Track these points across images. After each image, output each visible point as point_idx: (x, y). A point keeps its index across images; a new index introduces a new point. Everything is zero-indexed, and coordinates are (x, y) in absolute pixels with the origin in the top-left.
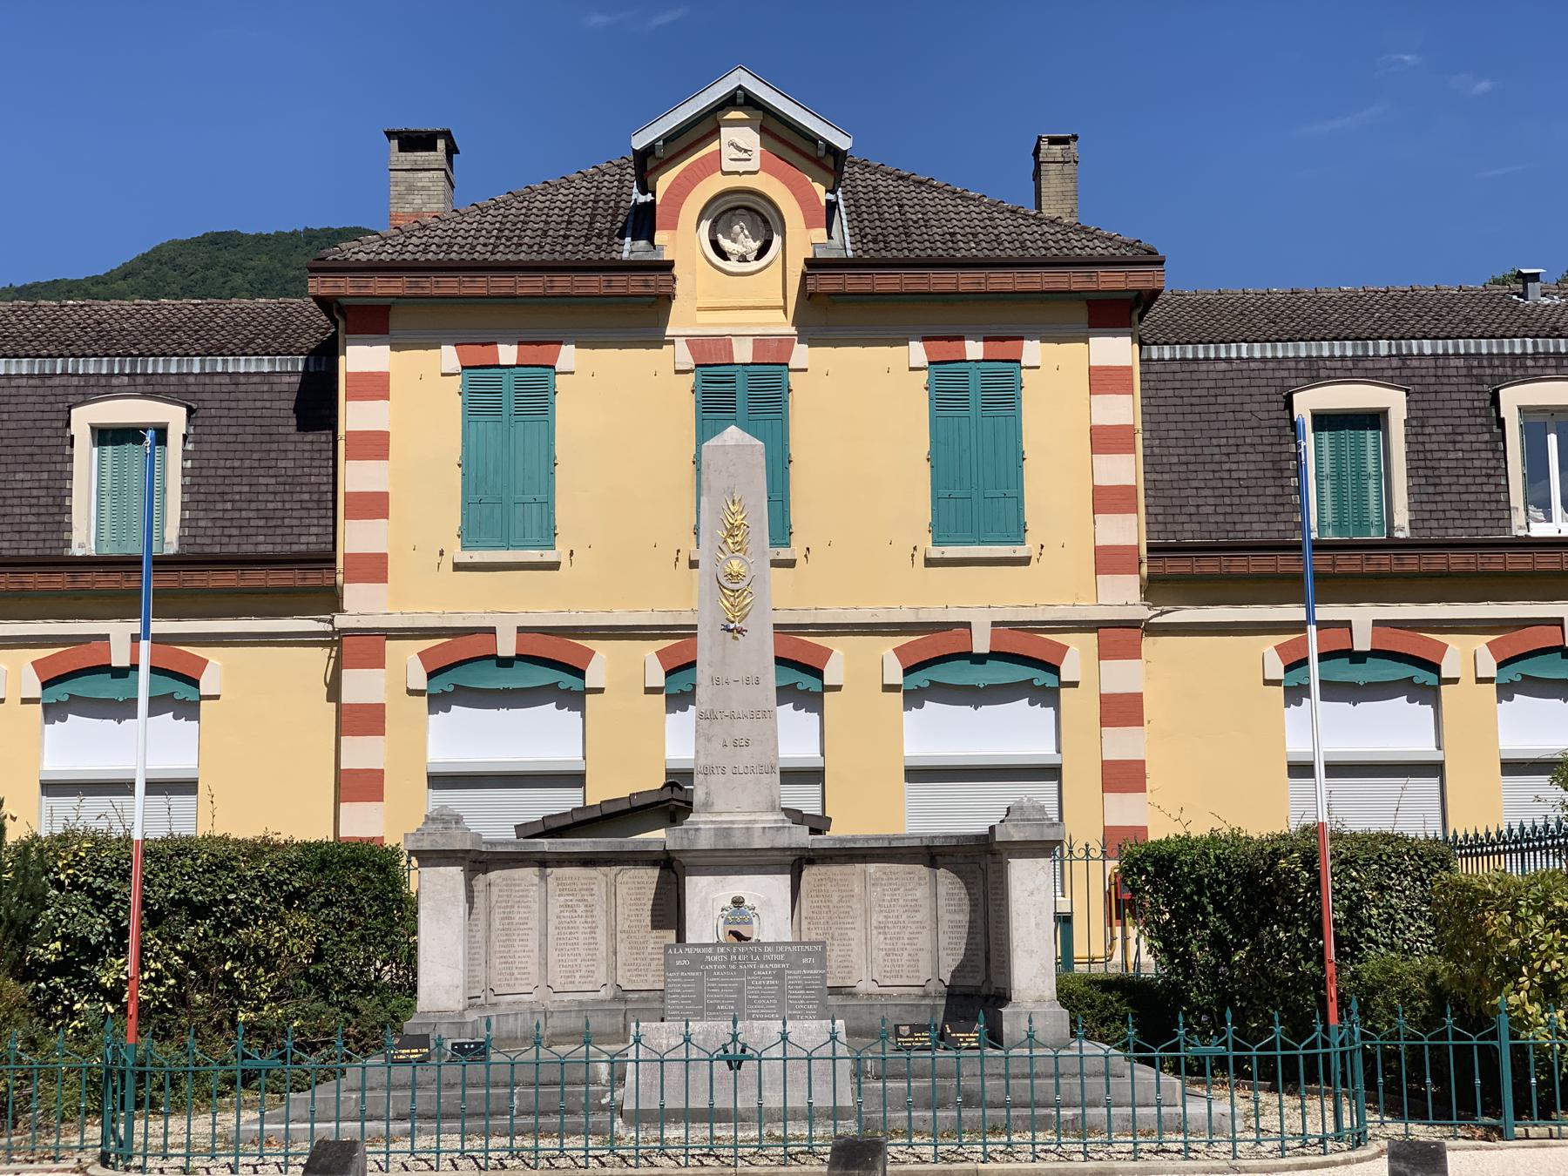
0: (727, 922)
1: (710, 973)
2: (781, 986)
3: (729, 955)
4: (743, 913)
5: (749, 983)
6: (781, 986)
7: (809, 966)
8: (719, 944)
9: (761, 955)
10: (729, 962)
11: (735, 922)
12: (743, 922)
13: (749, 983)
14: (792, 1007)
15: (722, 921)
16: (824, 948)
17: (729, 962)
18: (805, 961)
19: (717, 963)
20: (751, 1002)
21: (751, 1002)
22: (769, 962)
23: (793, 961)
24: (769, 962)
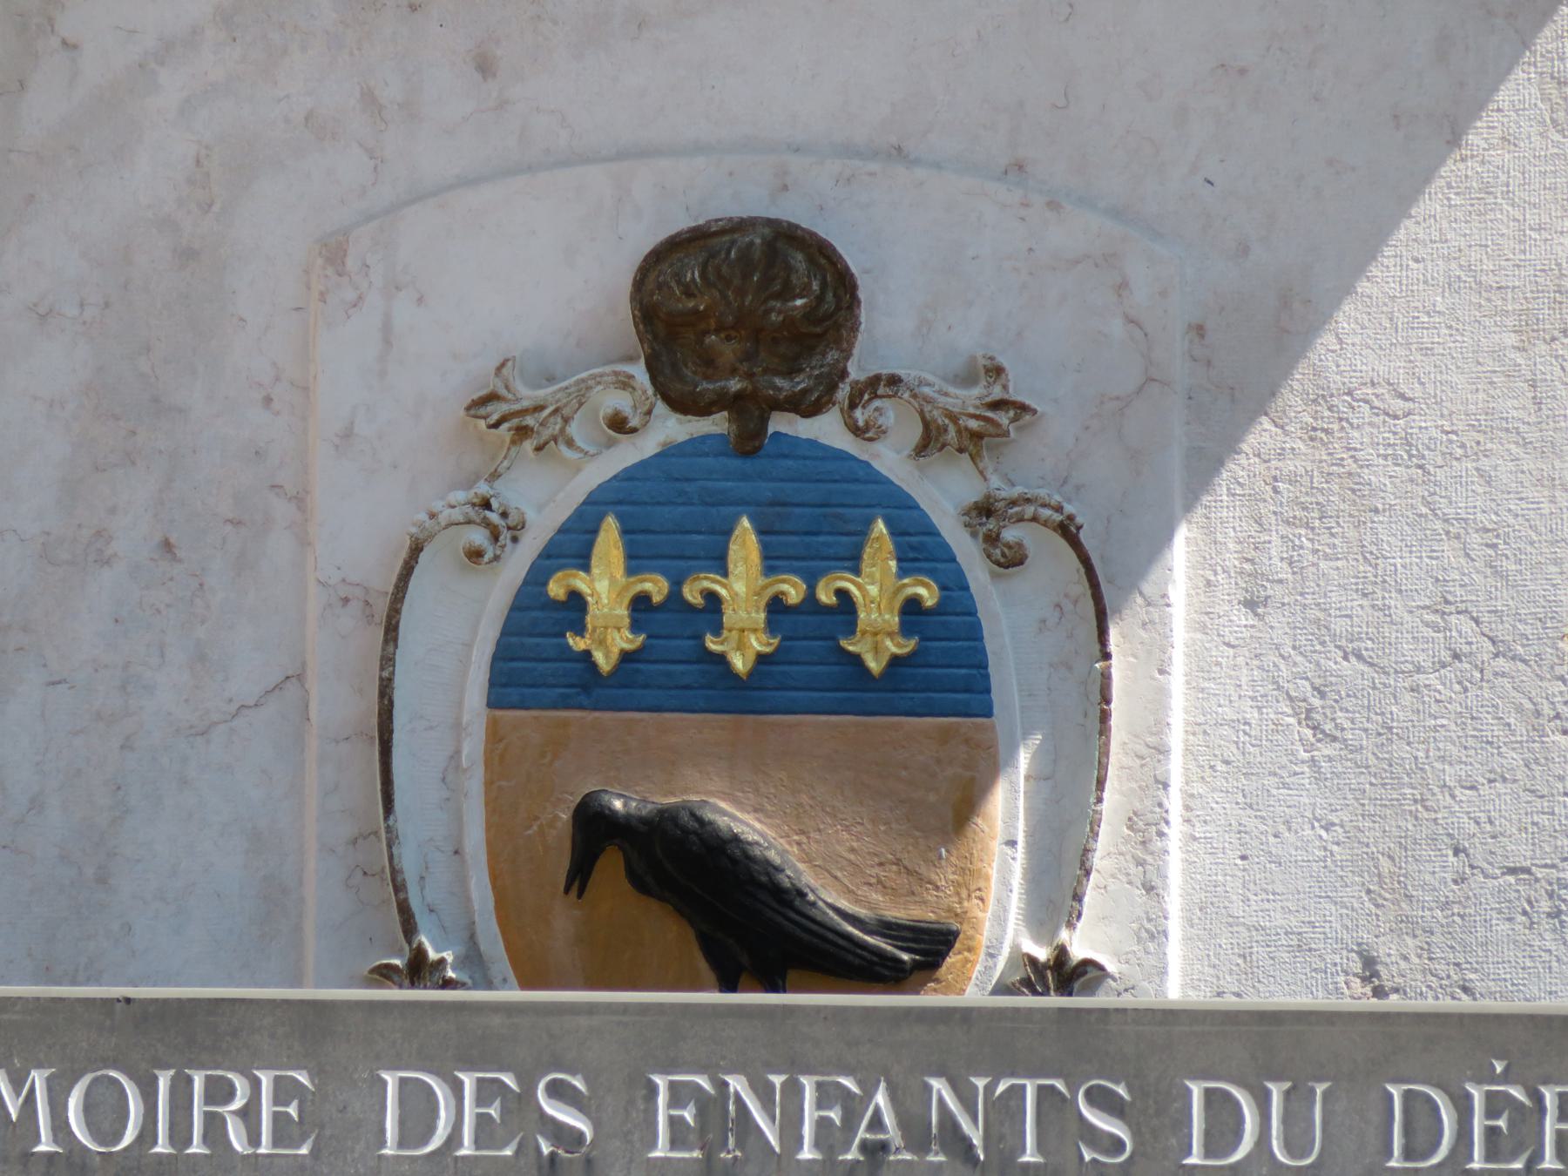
4: (821, 519)
11: (676, 664)
12: (813, 664)
15: (457, 628)
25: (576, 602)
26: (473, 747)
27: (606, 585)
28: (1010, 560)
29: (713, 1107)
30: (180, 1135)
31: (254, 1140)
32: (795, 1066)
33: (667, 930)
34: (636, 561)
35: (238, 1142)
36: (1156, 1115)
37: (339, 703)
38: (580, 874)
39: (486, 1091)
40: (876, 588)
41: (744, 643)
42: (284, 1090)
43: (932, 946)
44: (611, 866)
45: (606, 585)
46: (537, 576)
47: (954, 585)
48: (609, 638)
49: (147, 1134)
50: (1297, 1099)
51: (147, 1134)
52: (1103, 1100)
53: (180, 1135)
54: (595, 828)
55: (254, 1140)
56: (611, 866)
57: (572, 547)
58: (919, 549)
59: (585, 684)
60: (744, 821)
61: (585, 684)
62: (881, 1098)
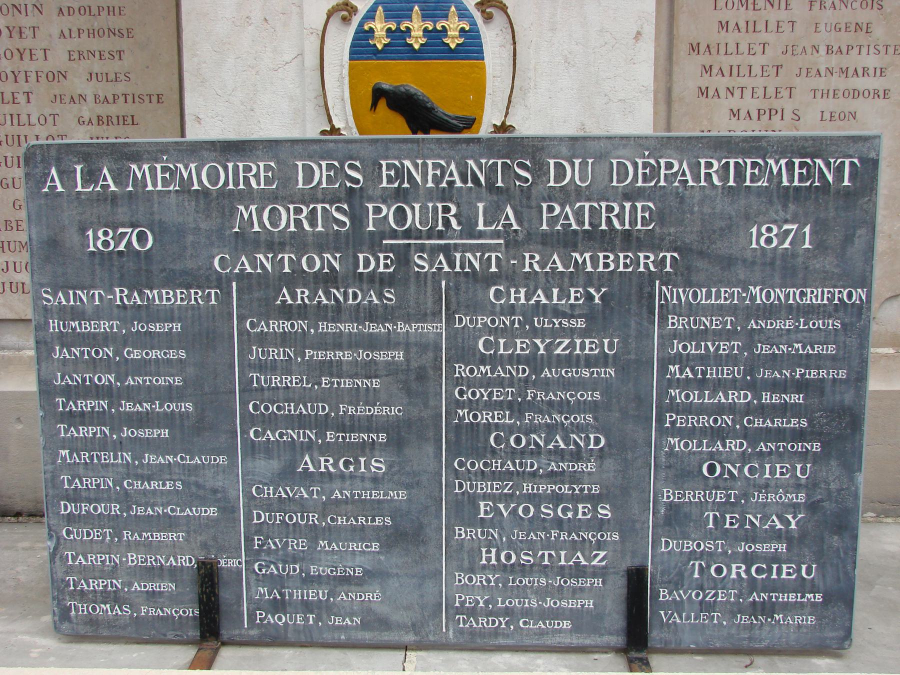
0: (362, 47)
1: (261, 292)
2: (631, 365)
3: (353, 197)
5: (462, 351)
6: (631, 365)
7: (785, 268)
8: (328, 144)
9: (526, 202)
10: (355, 240)
13: (462, 351)
14: (682, 472)
15: (341, 40)
16: (867, 171)
17: (355, 240)
18: (762, 237)
19: (298, 242)
20: (469, 440)
21: (469, 440)
22: (568, 241)
23: (697, 243)
24: (568, 241)
25: (371, 30)
26: (346, 72)
27: (380, 26)
28: (488, 18)
29: (400, 173)
30: (236, 184)
31: (259, 184)
32: (424, 157)
33: (399, 121)
34: (387, 18)
35: (254, 185)
36: (539, 170)
37: (312, 60)
38: (374, 105)
39: (330, 167)
40: (453, 25)
41: (417, 40)
42: (267, 168)
43: (469, 123)
44: (382, 104)
45: (380, 26)
46: (361, 25)
47: (474, 24)
48: (380, 40)
49: (226, 183)
50: (584, 164)
51: (226, 183)
52: (522, 166)
53: (236, 184)
54: (378, 94)
55: (259, 184)
56: (382, 104)
57: (370, 15)
58: (463, 14)
59: (376, 53)
60: (415, 86)
61: (376, 53)
62: (453, 167)
